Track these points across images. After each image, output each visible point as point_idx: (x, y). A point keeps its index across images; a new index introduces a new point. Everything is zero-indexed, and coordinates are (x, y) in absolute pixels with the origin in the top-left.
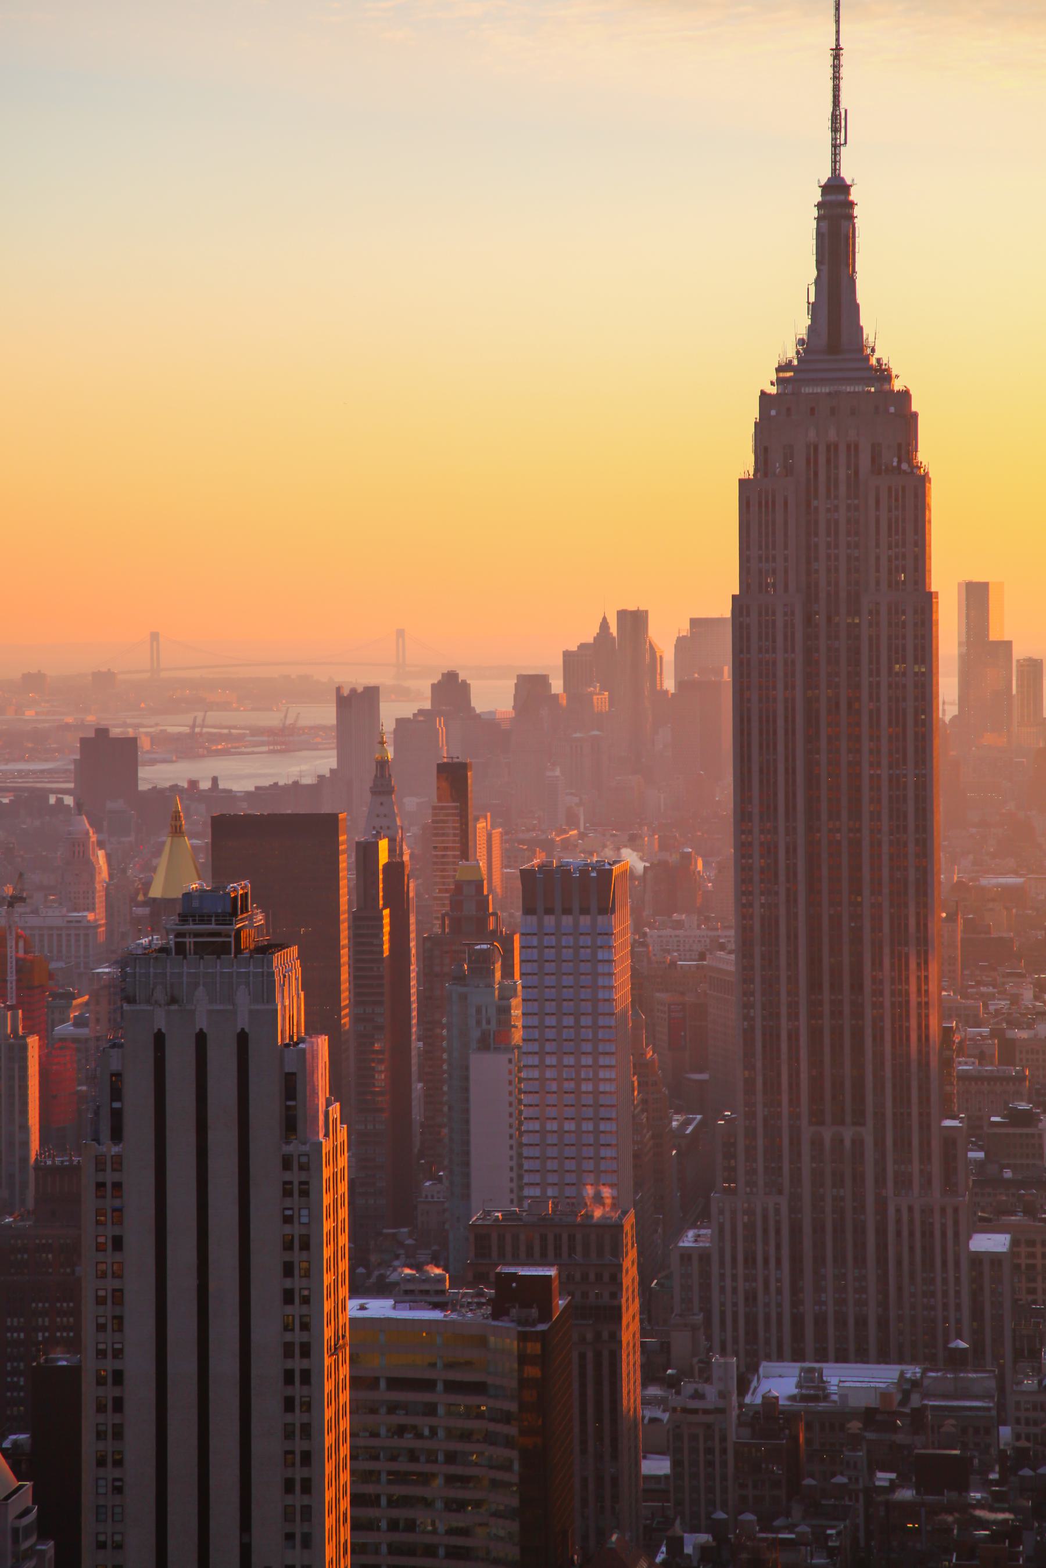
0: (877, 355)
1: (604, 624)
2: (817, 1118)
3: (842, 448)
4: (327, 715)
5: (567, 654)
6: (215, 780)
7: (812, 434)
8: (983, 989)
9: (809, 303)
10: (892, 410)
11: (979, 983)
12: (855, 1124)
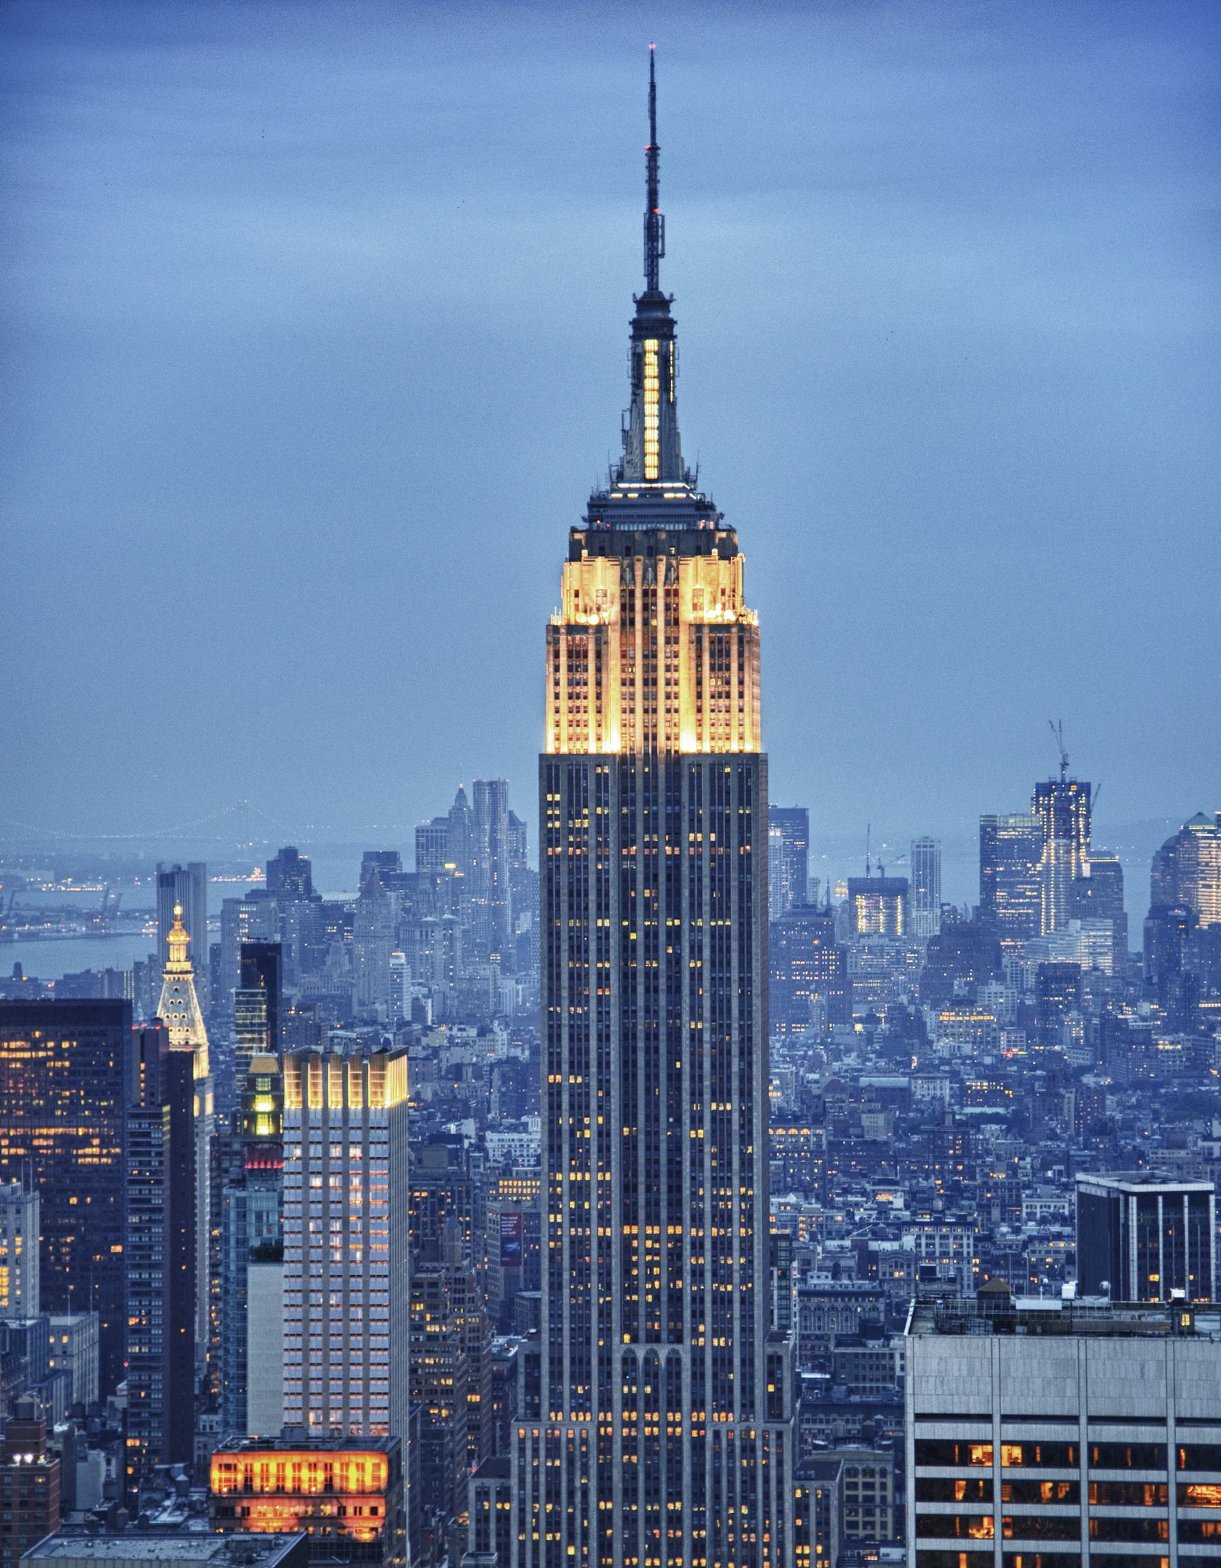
4: (146, 893)
8: (851, 1198)
9: (624, 431)
10: (715, 551)
11: (846, 1192)
12: (669, 1342)
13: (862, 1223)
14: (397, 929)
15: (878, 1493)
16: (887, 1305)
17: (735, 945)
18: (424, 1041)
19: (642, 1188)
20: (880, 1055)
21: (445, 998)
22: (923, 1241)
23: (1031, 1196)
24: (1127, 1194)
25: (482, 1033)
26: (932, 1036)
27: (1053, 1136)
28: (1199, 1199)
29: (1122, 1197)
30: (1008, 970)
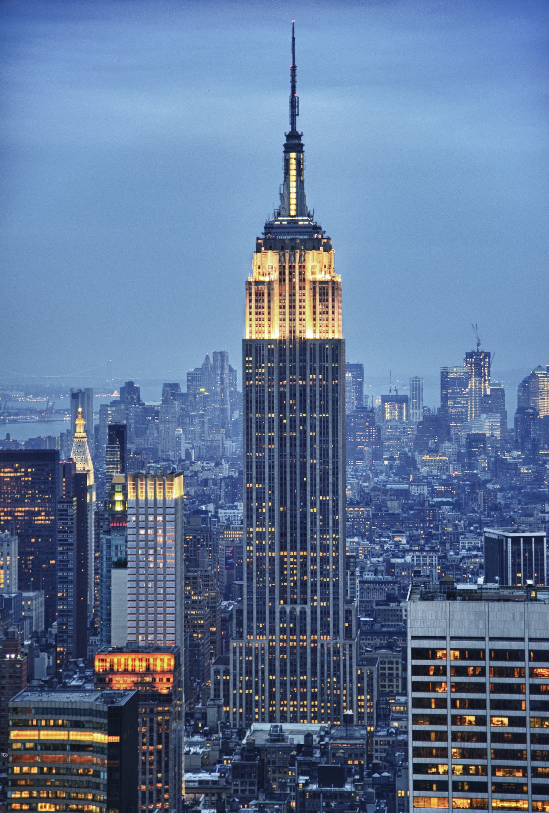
1: (207, 357)
4: (66, 402)
5: (189, 374)
8: (383, 539)
10: (321, 248)
11: (380, 536)
12: (301, 604)
13: (388, 550)
14: (179, 418)
15: (395, 672)
16: (399, 587)
17: (330, 425)
18: (191, 468)
19: (288, 535)
20: (396, 475)
21: (200, 449)
22: (415, 558)
23: (463, 538)
24: (507, 537)
25: (217, 465)
26: (419, 466)
27: (474, 511)
28: (539, 540)
29: (504, 539)
30: (453, 437)
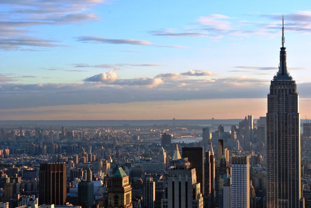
0: (290, 75)
1: (246, 118)
2: (280, 198)
3: (284, 90)
6: (183, 142)
7: (279, 87)
12: (286, 199)
25: (250, 152)
